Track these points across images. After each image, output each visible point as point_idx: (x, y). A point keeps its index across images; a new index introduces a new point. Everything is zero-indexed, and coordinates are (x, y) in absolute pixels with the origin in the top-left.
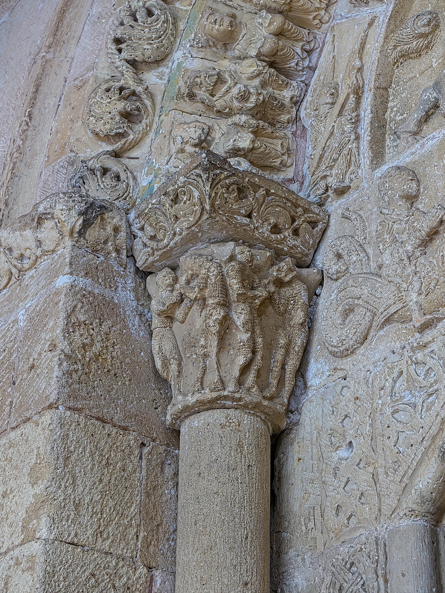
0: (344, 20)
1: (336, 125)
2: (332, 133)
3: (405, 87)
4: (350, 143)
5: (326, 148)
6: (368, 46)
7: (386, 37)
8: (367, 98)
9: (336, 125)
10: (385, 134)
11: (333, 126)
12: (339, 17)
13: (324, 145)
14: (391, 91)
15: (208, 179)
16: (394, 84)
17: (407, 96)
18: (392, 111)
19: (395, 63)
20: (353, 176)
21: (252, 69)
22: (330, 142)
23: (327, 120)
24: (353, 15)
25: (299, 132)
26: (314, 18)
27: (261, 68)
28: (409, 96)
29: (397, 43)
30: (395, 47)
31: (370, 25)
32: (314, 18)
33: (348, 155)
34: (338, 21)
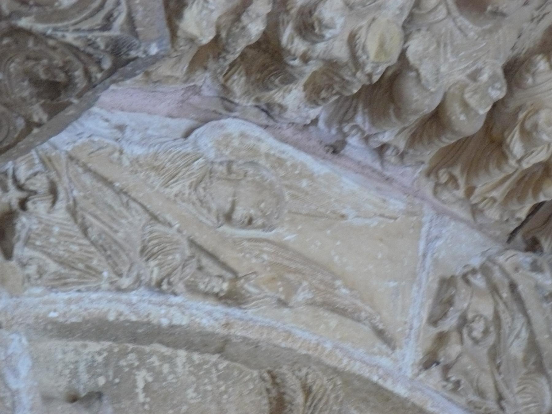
0: (422, 245)
1: (172, 231)
2: (154, 218)
3: (209, 398)
4: (113, 276)
5: (125, 199)
6: (333, 320)
7: (336, 371)
8: (210, 314)
9: (172, 231)
10: (114, 341)
11: (170, 225)
12: (435, 232)
13: (133, 194)
14: (214, 358)
15: (91, 44)
16: (227, 367)
17: (186, 402)
18: (164, 358)
19: (273, 377)
20: (32, 270)
21: (372, 48)
22: (137, 211)
23: (191, 207)
24: (424, 275)
25: (195, 100)
26: (453, 179)
27: (368, 69)
28: (184, 408)
29: (313, 399)
30: (307, 391)
31: (380, 334)
32: (453, 179)
33: (88, 267)
34: (425, 229)
